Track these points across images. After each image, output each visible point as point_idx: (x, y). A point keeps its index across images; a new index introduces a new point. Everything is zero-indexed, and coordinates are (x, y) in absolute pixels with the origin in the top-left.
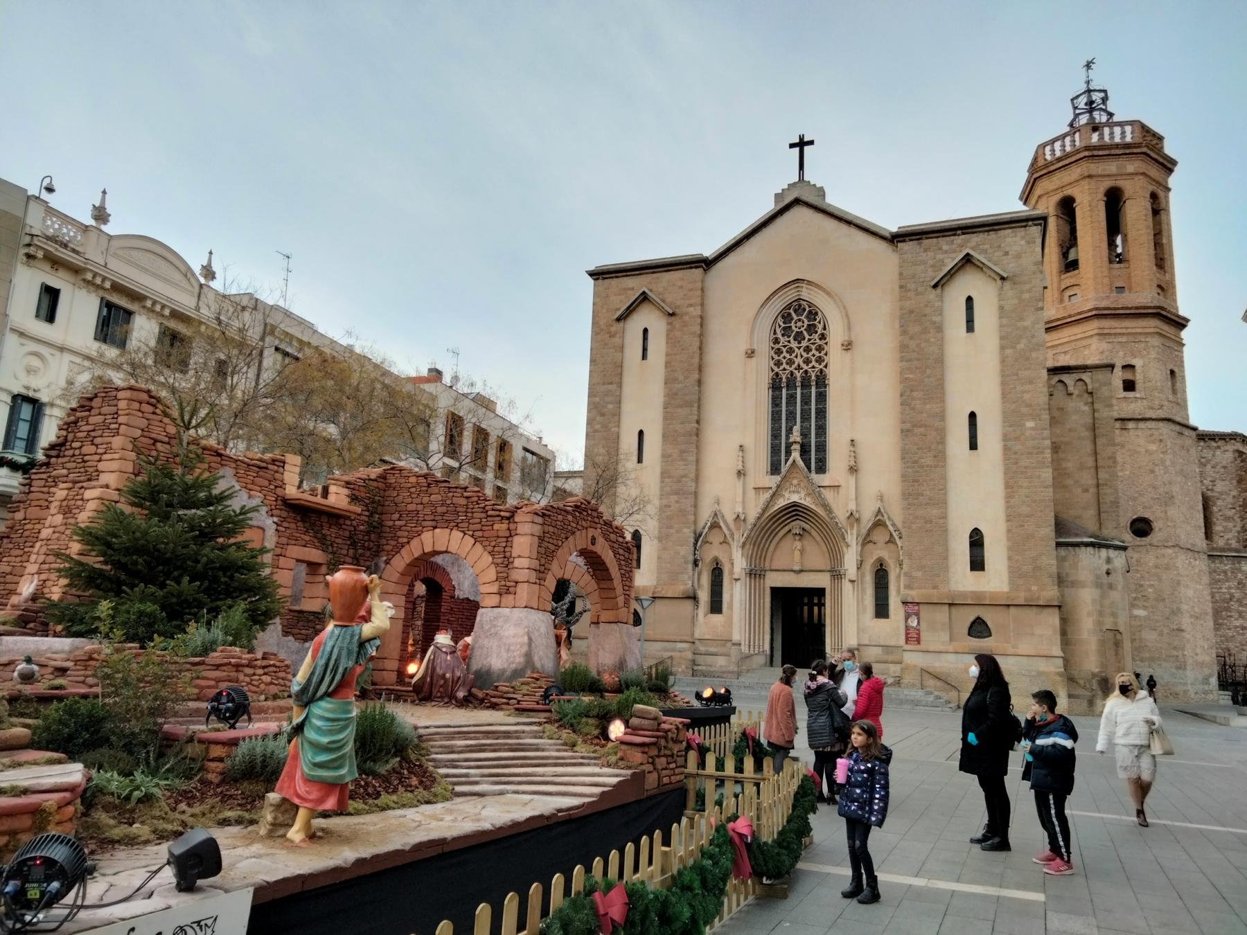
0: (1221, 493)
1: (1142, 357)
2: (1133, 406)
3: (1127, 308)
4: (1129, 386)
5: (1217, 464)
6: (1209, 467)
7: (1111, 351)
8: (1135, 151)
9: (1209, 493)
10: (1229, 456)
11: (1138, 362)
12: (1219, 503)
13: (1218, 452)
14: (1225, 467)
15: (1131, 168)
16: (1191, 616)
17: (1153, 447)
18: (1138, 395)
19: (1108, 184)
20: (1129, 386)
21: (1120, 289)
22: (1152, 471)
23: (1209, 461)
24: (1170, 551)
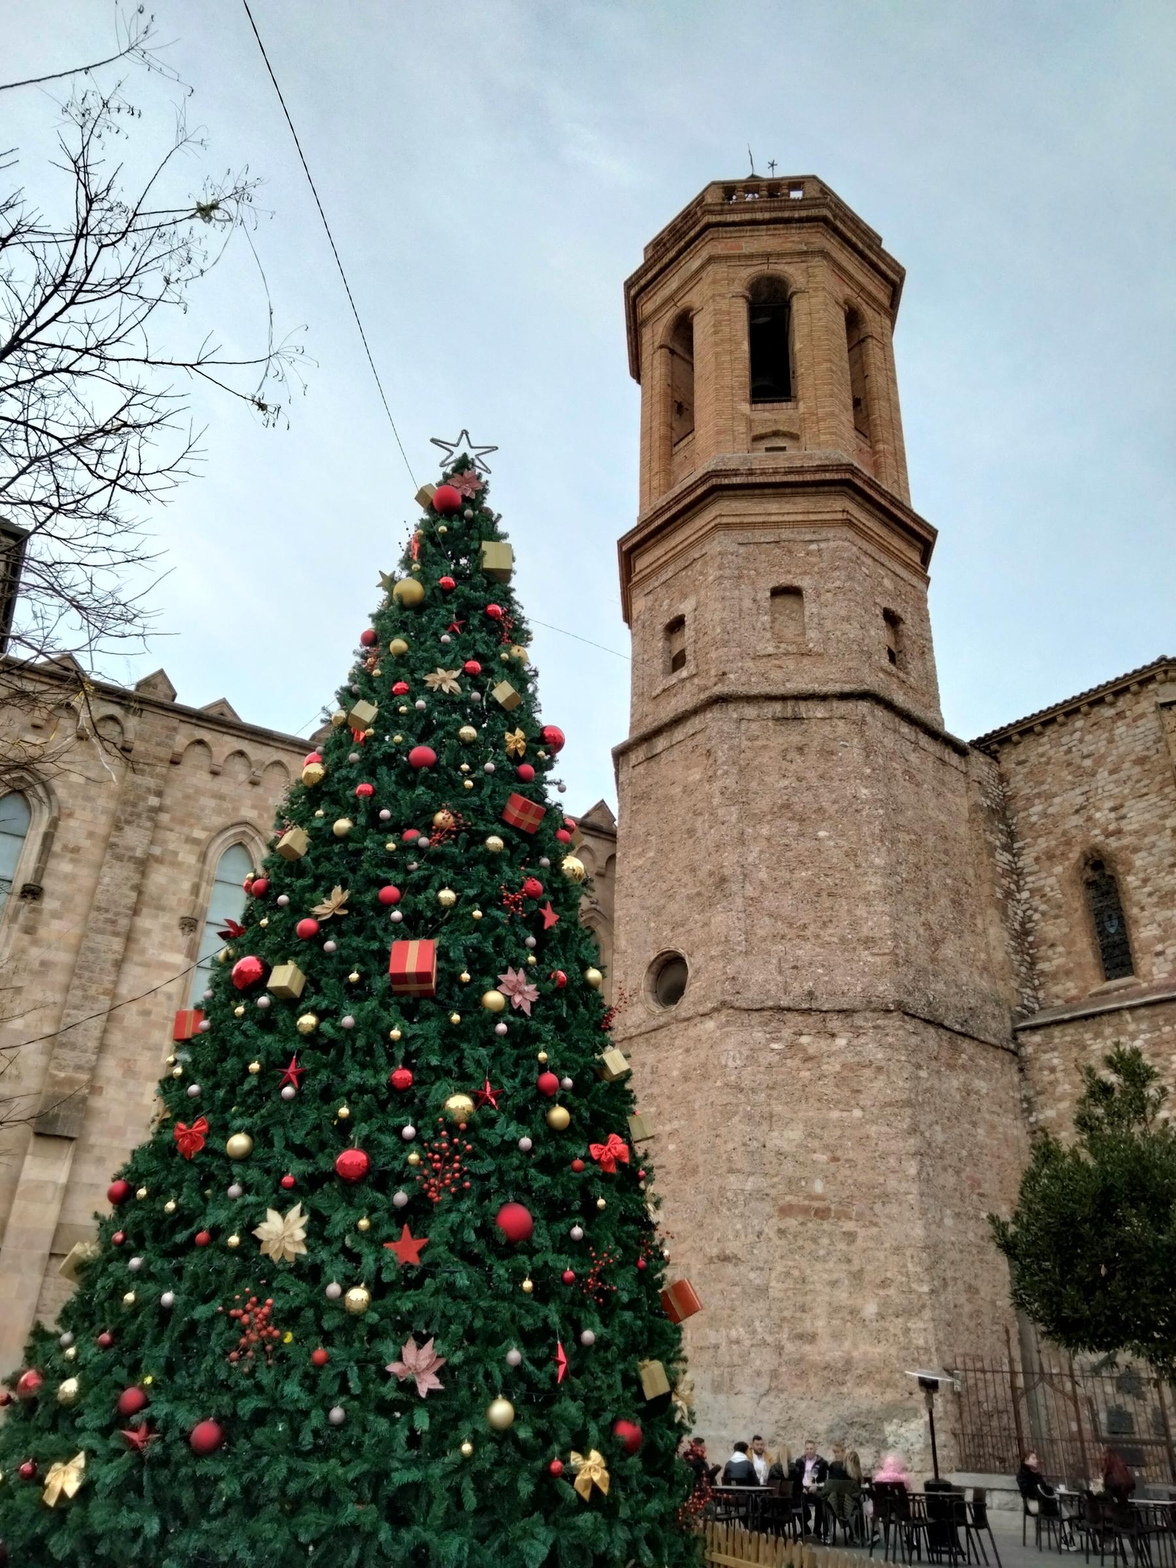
0: (1141, 833)
5: (1122, 759)
6: (1103, 774)
7: (651, 609)
8: (692, 233)
9: (1113, 843)
10: (1150, 723)
12: (1139, 860)
13: (1121, 729)
14: (1141, 761)
15: (696, 264)
16: (786, 1211)
17: (696, 775)
22: (691, 832)
23: (1099, 761)
24: (710, 1025)
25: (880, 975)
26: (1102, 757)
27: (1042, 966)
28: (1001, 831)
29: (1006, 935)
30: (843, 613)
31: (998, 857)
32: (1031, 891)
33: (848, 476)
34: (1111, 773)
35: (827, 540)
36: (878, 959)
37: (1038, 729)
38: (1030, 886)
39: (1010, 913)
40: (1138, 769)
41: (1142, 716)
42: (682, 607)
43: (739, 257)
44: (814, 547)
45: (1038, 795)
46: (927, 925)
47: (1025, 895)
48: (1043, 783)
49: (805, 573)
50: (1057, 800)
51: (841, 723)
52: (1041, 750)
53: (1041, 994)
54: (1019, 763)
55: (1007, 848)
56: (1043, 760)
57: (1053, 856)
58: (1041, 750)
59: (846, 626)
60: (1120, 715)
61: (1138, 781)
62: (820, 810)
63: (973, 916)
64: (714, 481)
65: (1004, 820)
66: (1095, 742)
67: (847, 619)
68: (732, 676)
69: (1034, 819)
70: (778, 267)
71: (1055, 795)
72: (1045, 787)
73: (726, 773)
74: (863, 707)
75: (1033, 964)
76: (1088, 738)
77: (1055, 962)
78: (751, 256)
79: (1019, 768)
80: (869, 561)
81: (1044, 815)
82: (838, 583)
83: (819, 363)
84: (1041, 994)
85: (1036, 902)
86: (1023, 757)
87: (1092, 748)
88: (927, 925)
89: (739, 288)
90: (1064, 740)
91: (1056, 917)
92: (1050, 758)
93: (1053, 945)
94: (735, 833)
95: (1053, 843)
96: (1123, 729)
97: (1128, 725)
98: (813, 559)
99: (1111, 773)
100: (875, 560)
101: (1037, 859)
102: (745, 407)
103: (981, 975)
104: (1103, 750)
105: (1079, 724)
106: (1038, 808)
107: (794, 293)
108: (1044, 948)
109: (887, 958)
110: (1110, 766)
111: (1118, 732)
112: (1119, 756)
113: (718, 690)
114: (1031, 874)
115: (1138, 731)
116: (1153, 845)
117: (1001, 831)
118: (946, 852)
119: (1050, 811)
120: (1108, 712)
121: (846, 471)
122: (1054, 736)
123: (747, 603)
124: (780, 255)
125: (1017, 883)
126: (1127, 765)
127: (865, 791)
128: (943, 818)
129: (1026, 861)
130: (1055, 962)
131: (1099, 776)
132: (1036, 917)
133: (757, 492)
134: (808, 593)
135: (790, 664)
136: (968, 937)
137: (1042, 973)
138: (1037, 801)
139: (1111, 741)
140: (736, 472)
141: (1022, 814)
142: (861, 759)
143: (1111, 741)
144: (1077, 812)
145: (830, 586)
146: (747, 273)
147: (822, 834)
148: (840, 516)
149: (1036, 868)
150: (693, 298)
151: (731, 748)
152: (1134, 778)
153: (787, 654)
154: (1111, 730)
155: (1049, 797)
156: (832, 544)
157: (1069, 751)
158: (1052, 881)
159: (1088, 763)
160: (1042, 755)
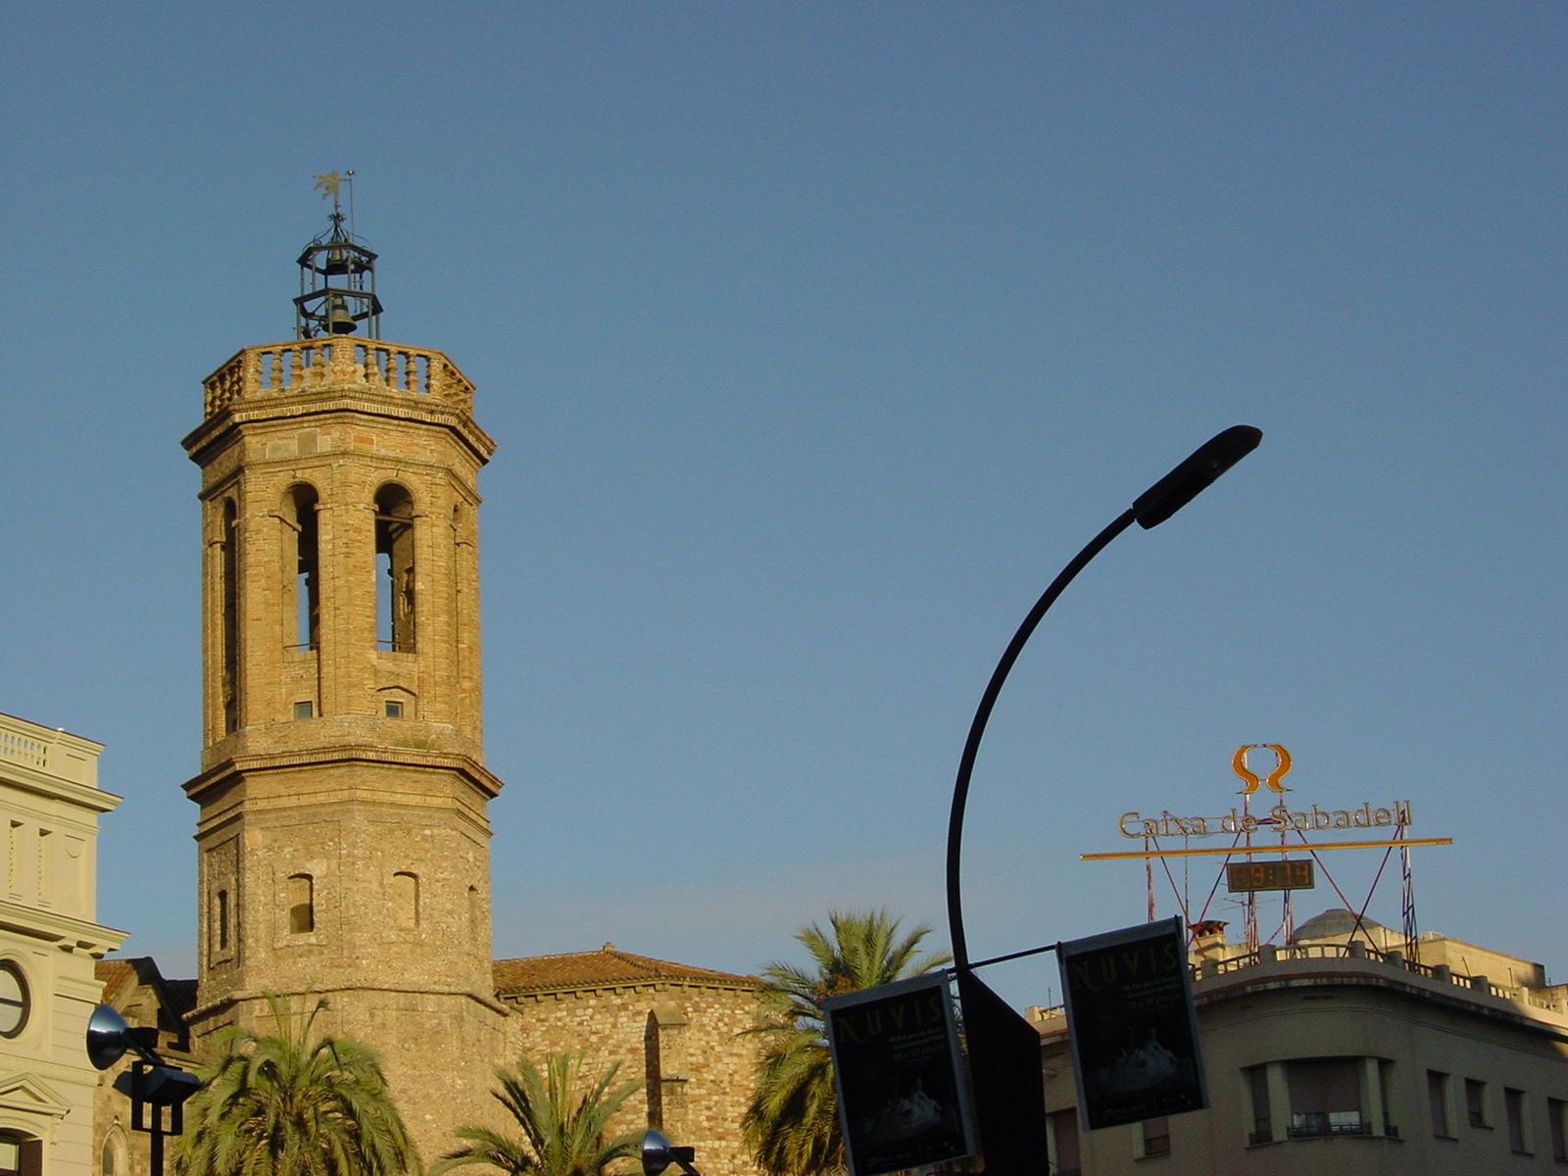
1: (327, 856)
2: (302, 962)
3: (292, 754)
4: (305, 919)
6: (604, 1052)
11: (317, 868)
15: (325, 442)
18: (313, 940)
19: (284, 479)
20: (305, 919)
21: (304, 708)
23: (604, 1040)
26: (608, 1037)
30: (449, 906)
34: (611, 1053)
40: (630, 1057)
41: (640, 1013)
42: (308, 865)
44: (427, 832)
48: (557, 1044)
49: (421, 860)
52: (559, 1014)
54: (539, 1020)
56: (559, 1024)
58: (559, 1014)
60: (624, 1007)
61: (630, 1067)
62: (427, 1096)
66: (602, 1023)
67: (450, 913)
68: (364, 962)
76: (598, 1017)
79: (539, 1024)
86: (543, 1016)
87: (600, 1027)
89: (368, 496)
90: (579, 1012)
92: (565, 1025)
96: (625, 1019)
97: (628, 1017)
98: (427, 846)
99: (611, 1053)
102: (373, 656)
104: (607, 1032)
105: (592, 1002)
110: (610, 1048)
111: (620, 1020)
112: (618, 1041)
115: (635, 1025)
116: (632, 1122)
120: (619, 1001)
122: (571, 1005)
123: (375, 886)
126: (622, 1051)
127: (459, 1082)
131: (601, 1053)
133: (386, 766)
134: (423, 880)
135: (407, 948)
139: (614, 1026)
140: (371, 747)
142: (457, 1053)
143: (614, 1026)
144: (580, 1078)
146: (377, 478)
147: (428, 1117)
150: (318, 479)
152: (627, 1064)
153: (405, 942)
154: (616, 1017)
157: (581, 1024)
159: (594, 1039)
160: (560, 1019)
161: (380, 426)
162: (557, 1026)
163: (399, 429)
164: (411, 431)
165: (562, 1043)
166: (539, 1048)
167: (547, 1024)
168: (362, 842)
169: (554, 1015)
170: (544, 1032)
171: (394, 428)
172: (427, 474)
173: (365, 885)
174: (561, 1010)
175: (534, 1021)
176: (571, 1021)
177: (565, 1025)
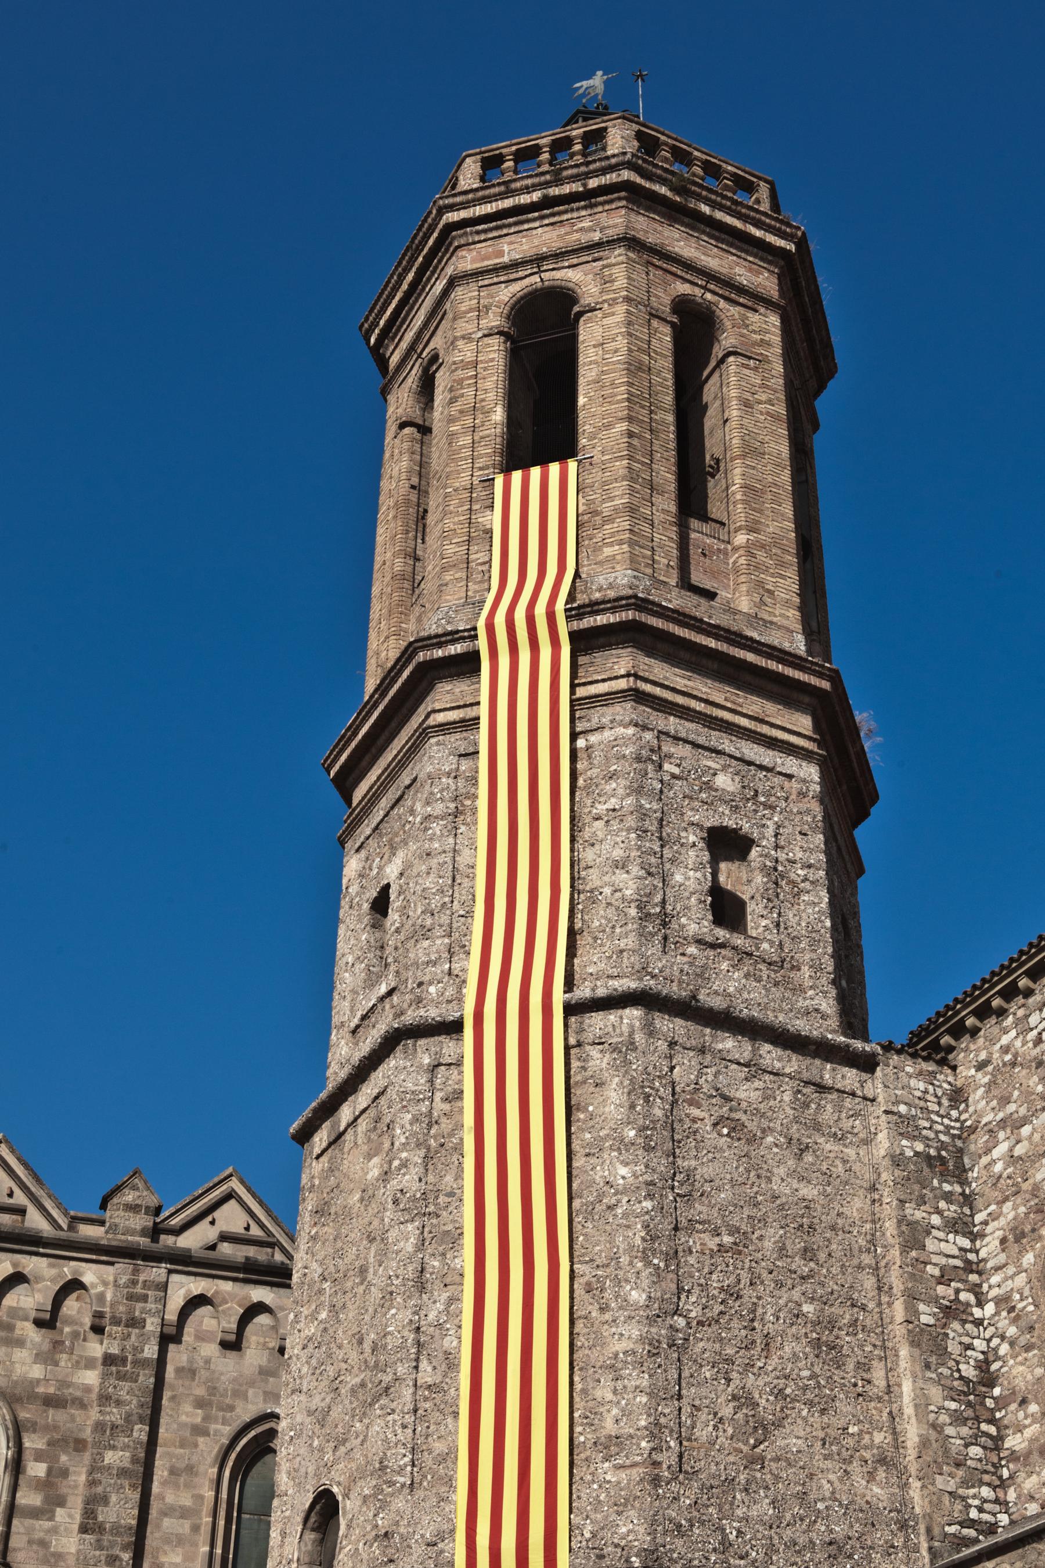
25: (621, 1507)
27: (1014, 1442)
28: (948, 1197)
29: (936, 1393)
31: (931, 1245)
32: (999, 1301)
33: (630, 615)
35: (600, 728)
36: (623, 1475)
37: (996, 1002)
38: (992, 1294)
39: (953, 1348)
43: (496, 270)
45: (1003, 1124)
46: (743, 1400)
47: (990, 1308)
50: (1026, 1130)
51: (594, 1052)
52: (1005, 1040)
53: (1011, 1495)
54: (981, 1066)
55: (960, 1226)
56: (1008, 1057)
57: (1023, 1235)
58: (1005, 1040)
59: (621, 876)
63: (863, 1366)
64: (421, 656)
65: (960, 1174)
68: (432, 989)
69: (998, 1167)
70: (557, 275)
71: (1024, 1121)
72: (1012, 1108)
73: (404, 1164)
74: (633, 1015)
75: (998, 1441)
77: (1028, 1433)
78: (515, 265)
80: (682, 751)
81: (1012, 1159)
82: (613, 802)
83: (608, 426)
84: (1011, 1495)
85: (1003, 1322)
86: (983, 1056)
88: (743, 1400)
91: (1028, 1348)
93: (1024, 1402)
94: (410, 1271)
95: (1022, 1209)
100: (695, 745)
101: (1003, 1241)
103: (871, 1476)
106: (1002, 1149)
107: (580, 314)
108: (1013, 1407)
109: (636, 1473)
113: (411, 1017)
114: (998, 1269)
117: (948, 1197)
118: (808, 1254)
119: (1019, 1150)
121: (627, 608)
122: (1021, 1013)
124: (558, 256)
125: (976, 1290)
127: (623, 1171)
128: (808, 1191)
129: (989, 1248)
130: (1028, 1433)
132: (1004, 1349)
136: (845, 1406)
137: (1014, 1456)
138: (1001, 1135)
141: (985, 1160)
145: (601, 808)
146: (507, 293)
148: (622, 684)
149: (1002, 1258)
151: (415, 1120)
155: (1013, 1124)
156: (607, 734)
158: (1021, 1280)
160: (1005, 1049)
161: (512, 230)
162: (1005, 1064)
163: (546, 221)
164: (565, 217)
165: (1016, 1093)
166: (984, 1121)
167: (990, 1068)
168: (442, 791)
169: (998, 1046)
170: (989, 1086)
171: (537, 224)
172: (594, 261)
173: (441, 859)
174: (1006, 1032)
175: (973, 1071)
176: (1023, 1045)
177: (1016, 1055)
